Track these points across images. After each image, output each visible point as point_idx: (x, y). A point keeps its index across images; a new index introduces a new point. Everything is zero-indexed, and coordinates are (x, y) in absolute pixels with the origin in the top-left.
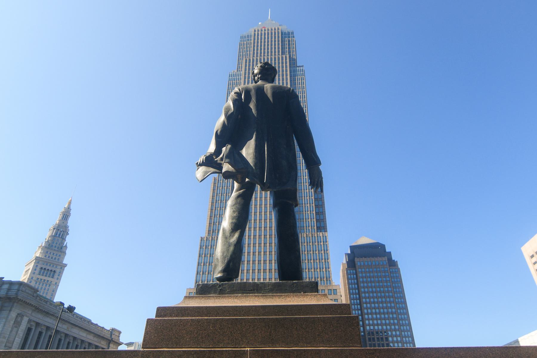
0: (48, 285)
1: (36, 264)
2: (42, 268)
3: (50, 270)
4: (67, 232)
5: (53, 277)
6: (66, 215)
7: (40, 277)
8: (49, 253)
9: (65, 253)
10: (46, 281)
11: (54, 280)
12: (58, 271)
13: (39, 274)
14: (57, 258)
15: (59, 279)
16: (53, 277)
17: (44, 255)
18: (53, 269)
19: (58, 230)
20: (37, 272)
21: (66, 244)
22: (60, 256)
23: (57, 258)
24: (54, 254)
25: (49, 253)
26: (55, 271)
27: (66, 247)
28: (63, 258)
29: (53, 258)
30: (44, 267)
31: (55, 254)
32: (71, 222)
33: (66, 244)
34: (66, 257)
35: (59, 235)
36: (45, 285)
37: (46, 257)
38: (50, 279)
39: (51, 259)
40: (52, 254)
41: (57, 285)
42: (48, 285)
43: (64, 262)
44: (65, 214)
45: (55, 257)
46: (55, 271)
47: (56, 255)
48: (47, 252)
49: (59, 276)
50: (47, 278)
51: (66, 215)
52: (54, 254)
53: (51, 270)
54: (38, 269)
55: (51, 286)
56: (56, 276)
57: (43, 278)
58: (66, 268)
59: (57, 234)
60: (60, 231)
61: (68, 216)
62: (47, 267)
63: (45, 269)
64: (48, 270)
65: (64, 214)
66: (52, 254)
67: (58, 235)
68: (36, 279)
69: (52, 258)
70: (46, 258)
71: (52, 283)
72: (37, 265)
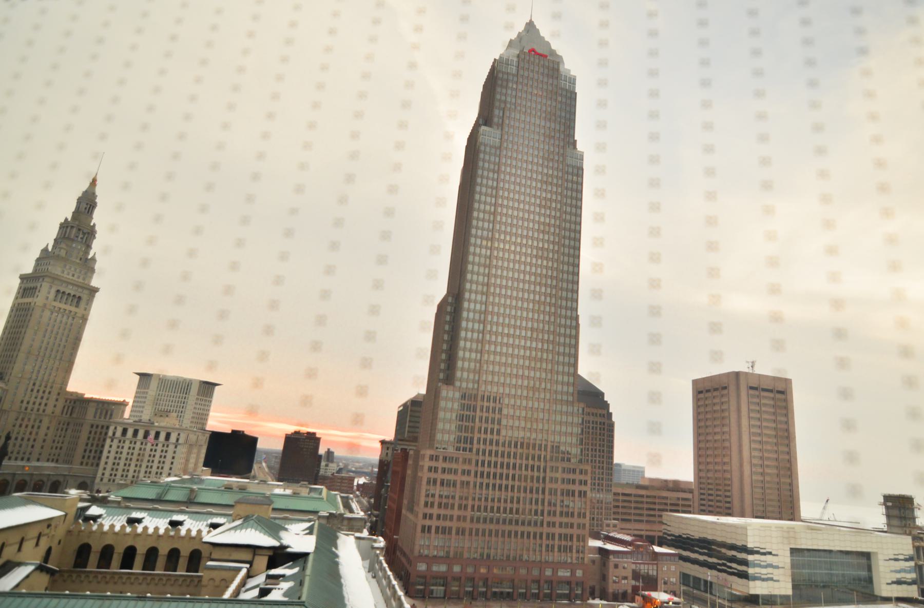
0: (71, 318)
2: (58, 291)
3: (72, 295)
4: (94, 236)
5: (77, 306)
6: (91, 205)
7: (57, 304)
9: (92, 271)
10: (67, 312)
11: (80, 311)
12: (85, 298)
13: (55, 300)
15: (87, 309)
16: (77, 306)
19: (79, 230)
20: (52, 296)
21: (95, 254)
22: (86, 274)
25: (67, 267)
26: (79, 298)
27: (93, 260)
28: (91, 277)
29: (75, 276)
30: (62, 289)
31: (78, 270)
32: (99, 218)
33: (95, 254)
34: (95, 276)
36: (65, 317)
38: (73, 309)
39: (71, 278)
40: (73, 269)
41: (84, 319)
42: (71, 318)
43: (94, 283)
46: (79, 298)
47: (80, 272)
49: (87, 304)
50: (68, 307)
53: (74, 296)
54: (53, 291)
55: (75, 320)
56: (83, 304)
57: (63, 306)
58: (97, 294)
59: (77, 237)
60: (83, 232)
61: (93, 207)
63: (64, 293)
64: (69, 294)
66: (73, 269)
69: (73, 275)
71: (77, 315)
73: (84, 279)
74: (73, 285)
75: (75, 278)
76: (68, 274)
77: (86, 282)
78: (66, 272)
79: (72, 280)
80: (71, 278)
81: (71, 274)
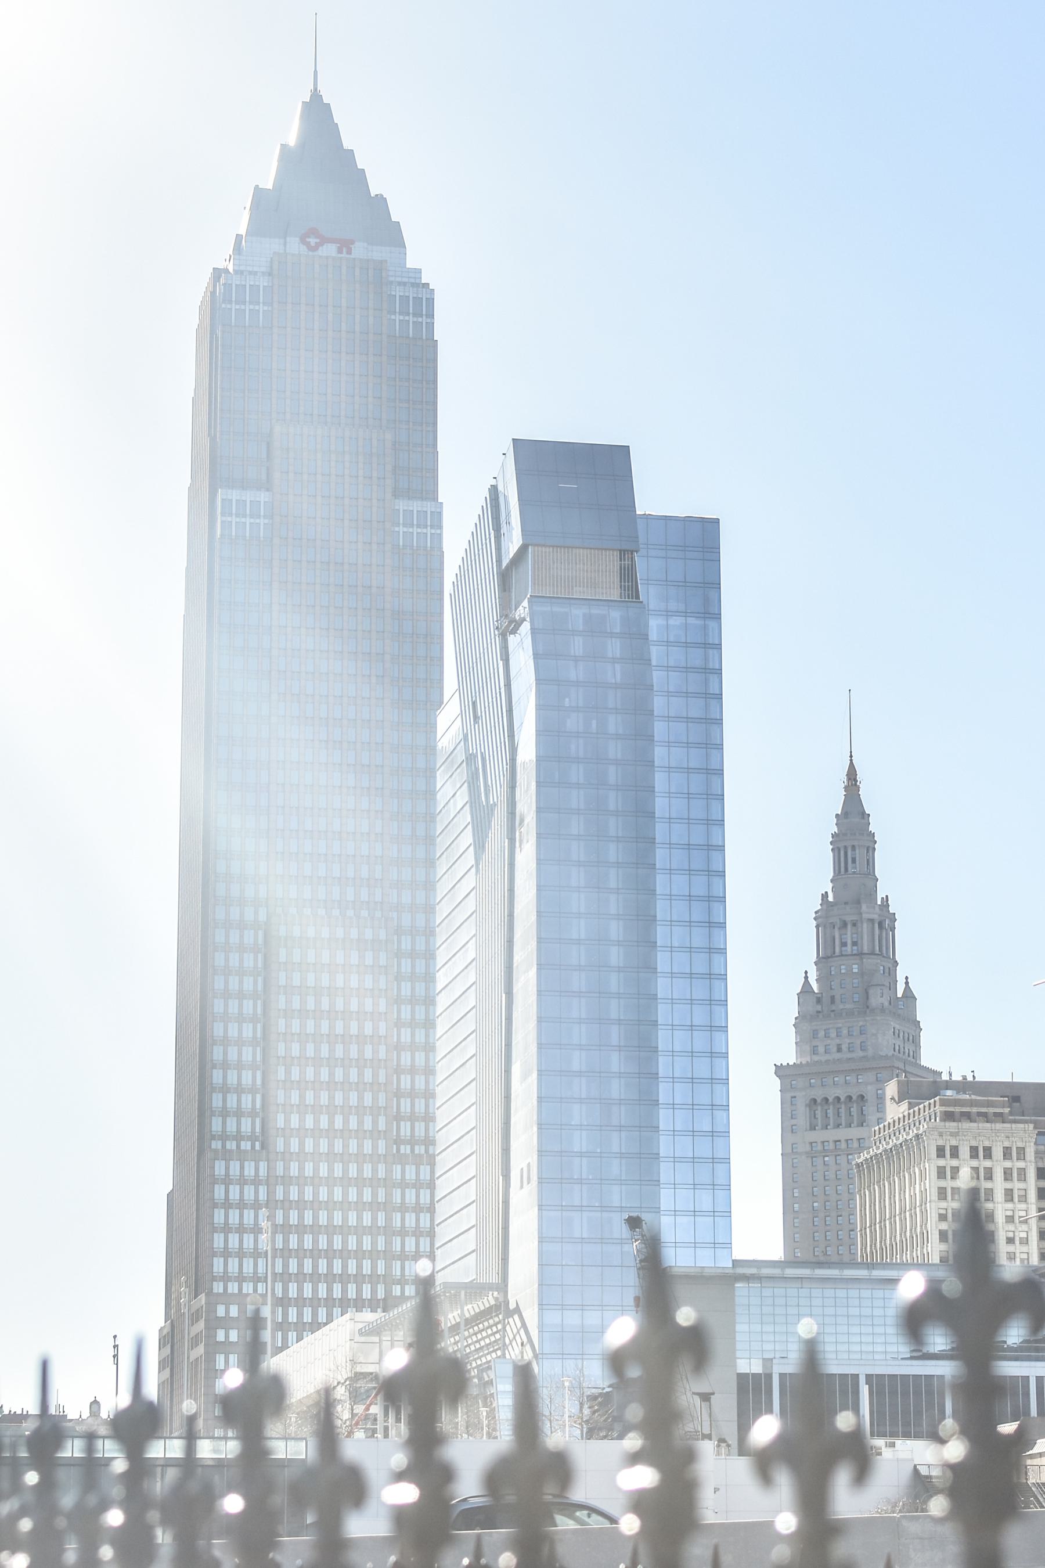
1: (789, 1095)
6: (846, 848)
7: (819, 1135)
8: (822, 1034)
13: (813, 1128)
17: (807, 1048)
18: (854, 1093)
20: (802, 1119)
25: (822, 1034)
29: (844, 1047)
30: (819, 1094)
39: (838, 1056)
40: (833, 1034)
44: (841, 845)
45: (848, 1041)
46: (862, 1097)
47: (850, 1035)
48: (815, 1034)
51: (846, 848)
53: (850, 1098)
57: (831, 1134)
61: (853, 848)
62: (832, 1093)
67: (837, 950)
68: (808, 1148)
69: (839, 1050)
70: (816, 1058)
72: (793, 1094)
73: (863, 1048)
77: (870, 1052)
78: (821, 1049)
80: (838, 1056)
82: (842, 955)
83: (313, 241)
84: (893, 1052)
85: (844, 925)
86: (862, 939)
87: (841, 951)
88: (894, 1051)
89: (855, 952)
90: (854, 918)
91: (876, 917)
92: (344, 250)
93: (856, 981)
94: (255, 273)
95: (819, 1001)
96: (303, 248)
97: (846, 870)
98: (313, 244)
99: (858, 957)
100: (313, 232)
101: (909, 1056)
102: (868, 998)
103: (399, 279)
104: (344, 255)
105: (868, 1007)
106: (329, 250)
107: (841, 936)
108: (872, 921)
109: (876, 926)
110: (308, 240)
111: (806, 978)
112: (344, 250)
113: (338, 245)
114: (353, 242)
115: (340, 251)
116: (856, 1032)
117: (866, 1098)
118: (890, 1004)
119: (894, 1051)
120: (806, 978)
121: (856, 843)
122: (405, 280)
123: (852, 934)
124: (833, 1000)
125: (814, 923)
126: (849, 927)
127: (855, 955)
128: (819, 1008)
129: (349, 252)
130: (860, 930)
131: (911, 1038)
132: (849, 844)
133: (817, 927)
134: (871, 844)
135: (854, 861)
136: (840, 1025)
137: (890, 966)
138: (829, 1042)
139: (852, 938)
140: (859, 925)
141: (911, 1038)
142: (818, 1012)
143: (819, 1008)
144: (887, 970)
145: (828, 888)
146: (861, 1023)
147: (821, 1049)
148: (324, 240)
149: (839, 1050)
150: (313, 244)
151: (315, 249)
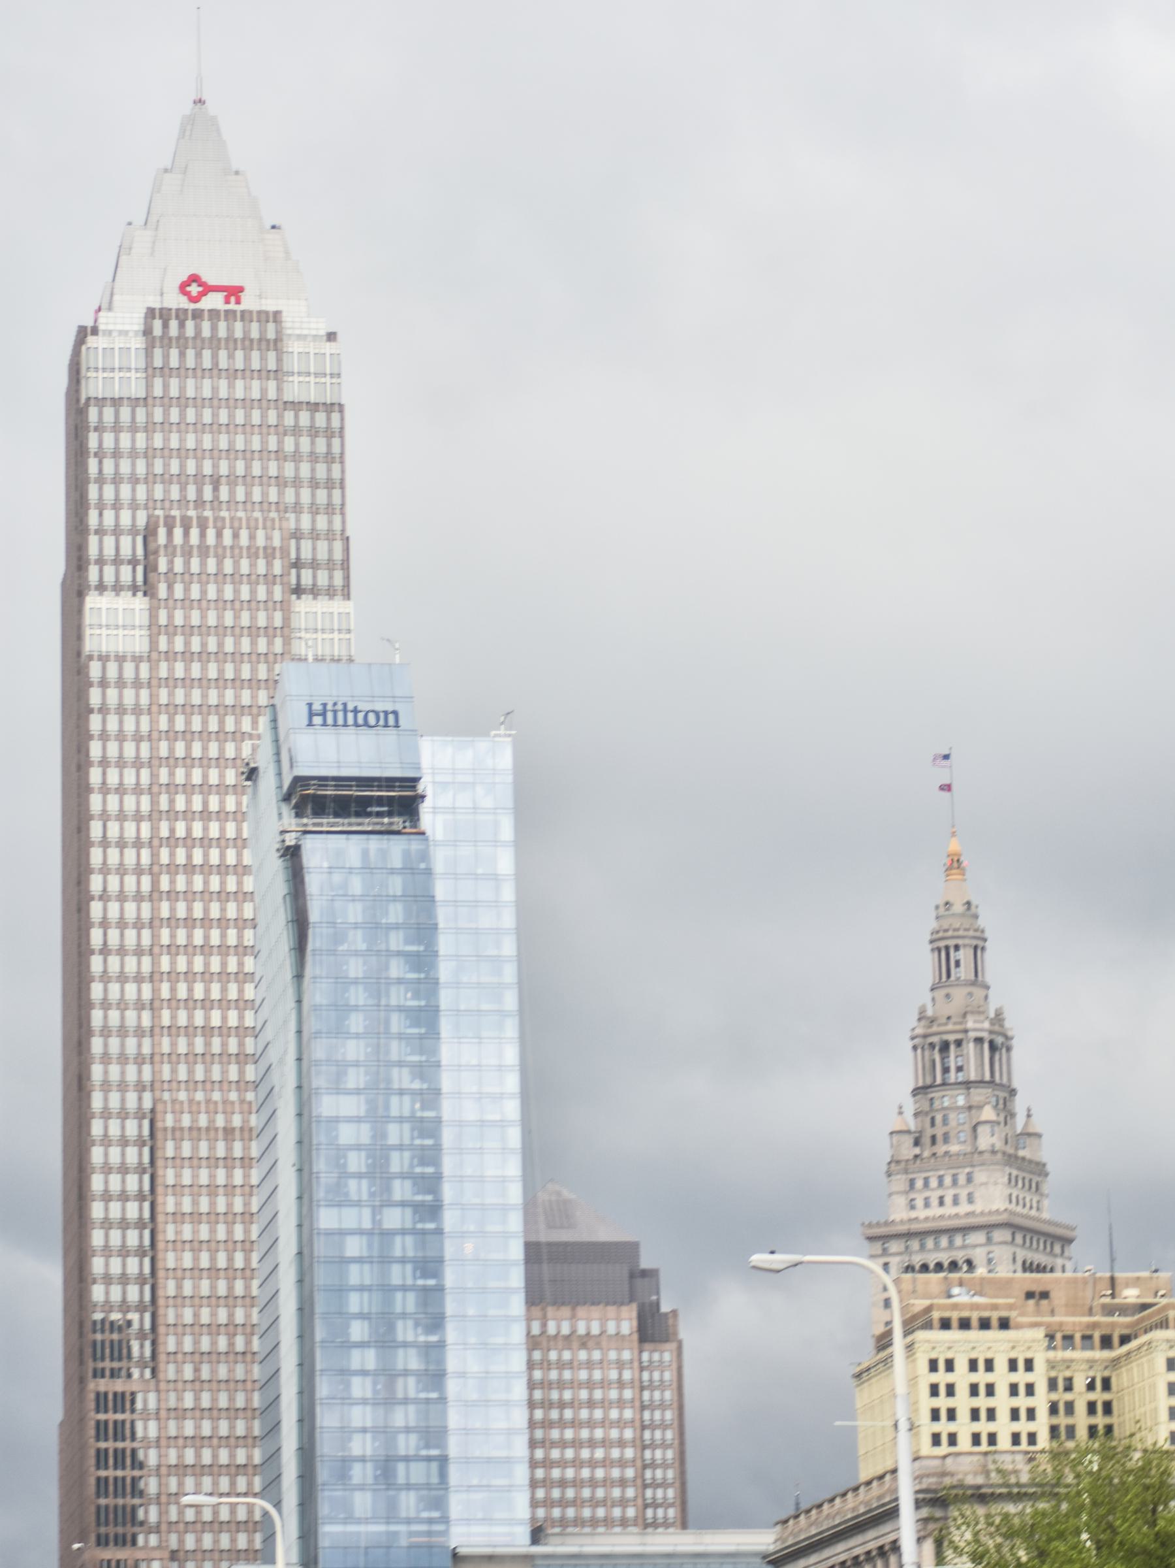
14: (963, 1194)
22: (969, 1179)
23: (963, 1194)
24: (941, 1179)
25: (919, 1184)
29: (948, 1200)
31: (948, 1180)
35: (946, 1070)
37: (913, 1207)
44: (942, 944)
47: (955, 1182)
51: (947, 948)
52: (941, 1179)
61: (957, 948)
65: (939, 950)
66: (934, 1183)
69: (941, 1202)
70: (913, 1214)
73: (970, 1199)
74: (937, 1233)
75: (949, 1210)
76: (927, 1205)
77: (978, 1207)
78: (919, 1203)
79: (942, 1217)
81: (934, 1202)
82: (944, 1084)
83: (194, 289)
84: (1006, 1205)
85: (945, 1047)
86: (968, 1062)
87: (944, 1079)
88: (1010, 1202)
89: (960, 1079)
90: (959, 1036)
91: (985, 1035)
92: (233, 299)
93: (961, 1116)
94: (126, 333)
95: (917, 1143)
96: (183, 303)
97: (949, 976)
98: (194, 294)
99: (963, 1086)
100: (194, 279)
101: (1031, 1208)
102: (975, 1138)
103: (298, 332)
104: (232, 306)
105: (976, 1149)
106: (214, 301)
107: (943, 1059)
108: (979, 1040)
109: (986, 1046)
110: (188, 289)
111: (901, 1113)
112: (233, 299)
113: (225, 294)
114: (241, 289)
115: (227, 302)
116: (962, 1179)
117: (974, 1264)
118: (1006, 1143)
119: (1010, 1202)
120: (901, 1113)
121: (960, 942)
122: (305, 332)
123: (957, 1057)
124: (933, 1139)
125: (910, 1044)
126: (952, 1047)
127: (960, 1083)
128: (917, 1151)
129: (238, 302)
130: (965, 1052)
131: (1034, 1185)
132: (951, 943)
133: (915, 1048)
134: (980, 943)
135: (958, 964)
136: (941, 1173)
137: (1006, 1095)
138: (927, 1194)
139: (956, 1062)
140: (964, 1043)
141: (1034, 1185)
142: (916, 1156)
143: (917, 1151)
144: (1001, 1102)
145: (925, 997)
146: (968, 1170)
147: (919, 1203)
148: (207, 289)
149: (941, 1202)
150: (194, 294)
151: (195, 300)
